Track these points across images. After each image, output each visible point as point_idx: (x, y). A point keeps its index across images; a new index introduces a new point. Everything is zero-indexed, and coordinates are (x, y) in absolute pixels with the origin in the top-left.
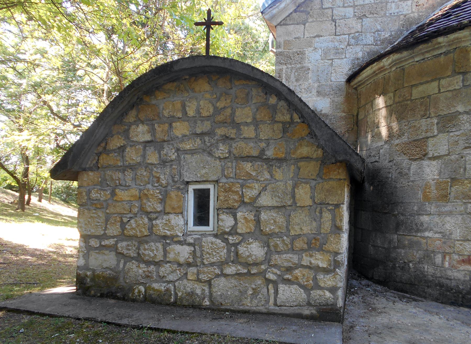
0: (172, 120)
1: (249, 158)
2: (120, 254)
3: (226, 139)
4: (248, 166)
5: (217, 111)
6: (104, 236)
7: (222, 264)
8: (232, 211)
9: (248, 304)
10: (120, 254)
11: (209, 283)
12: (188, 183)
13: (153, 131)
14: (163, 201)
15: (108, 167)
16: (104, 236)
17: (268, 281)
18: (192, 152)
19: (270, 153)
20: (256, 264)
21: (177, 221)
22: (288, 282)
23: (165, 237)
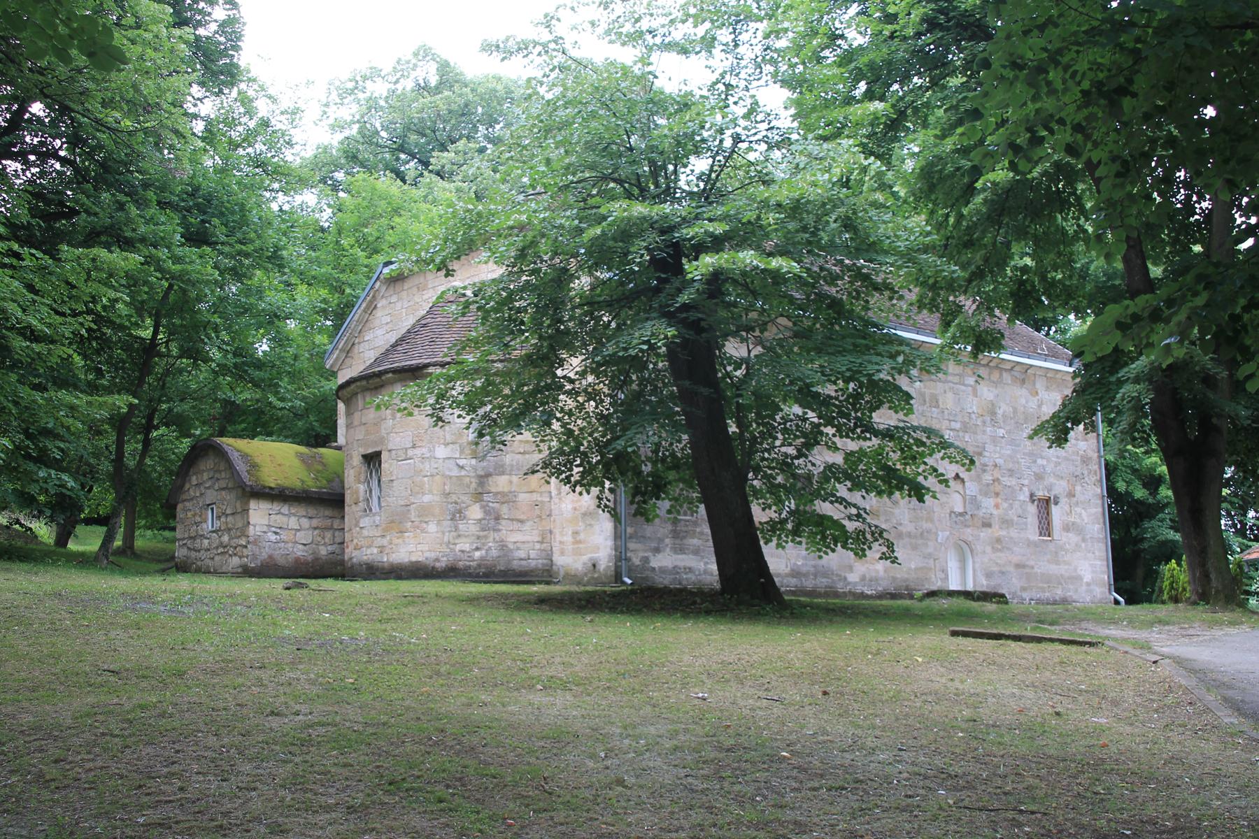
0: (204, 471)
1: (223, 489)
2: (188, 548)
3: (218, 479)
4: (224, 493)
5: (215, 464)
6: (184, 539)
7: (217, 548)
8: (219, 518)
9: (224, 569)
10: (188, 548)
11: (213, 558)
12: (209, 505)
13: (197, 479)
14: (200, 516)
15: (185, 500)
16: (184, 539)
17: (231, 556)
18: (208, 488)
19: (230, 486)
20: (226, 547)
21: (204, 526)
22: (235, 555)
23: (201, 536)
